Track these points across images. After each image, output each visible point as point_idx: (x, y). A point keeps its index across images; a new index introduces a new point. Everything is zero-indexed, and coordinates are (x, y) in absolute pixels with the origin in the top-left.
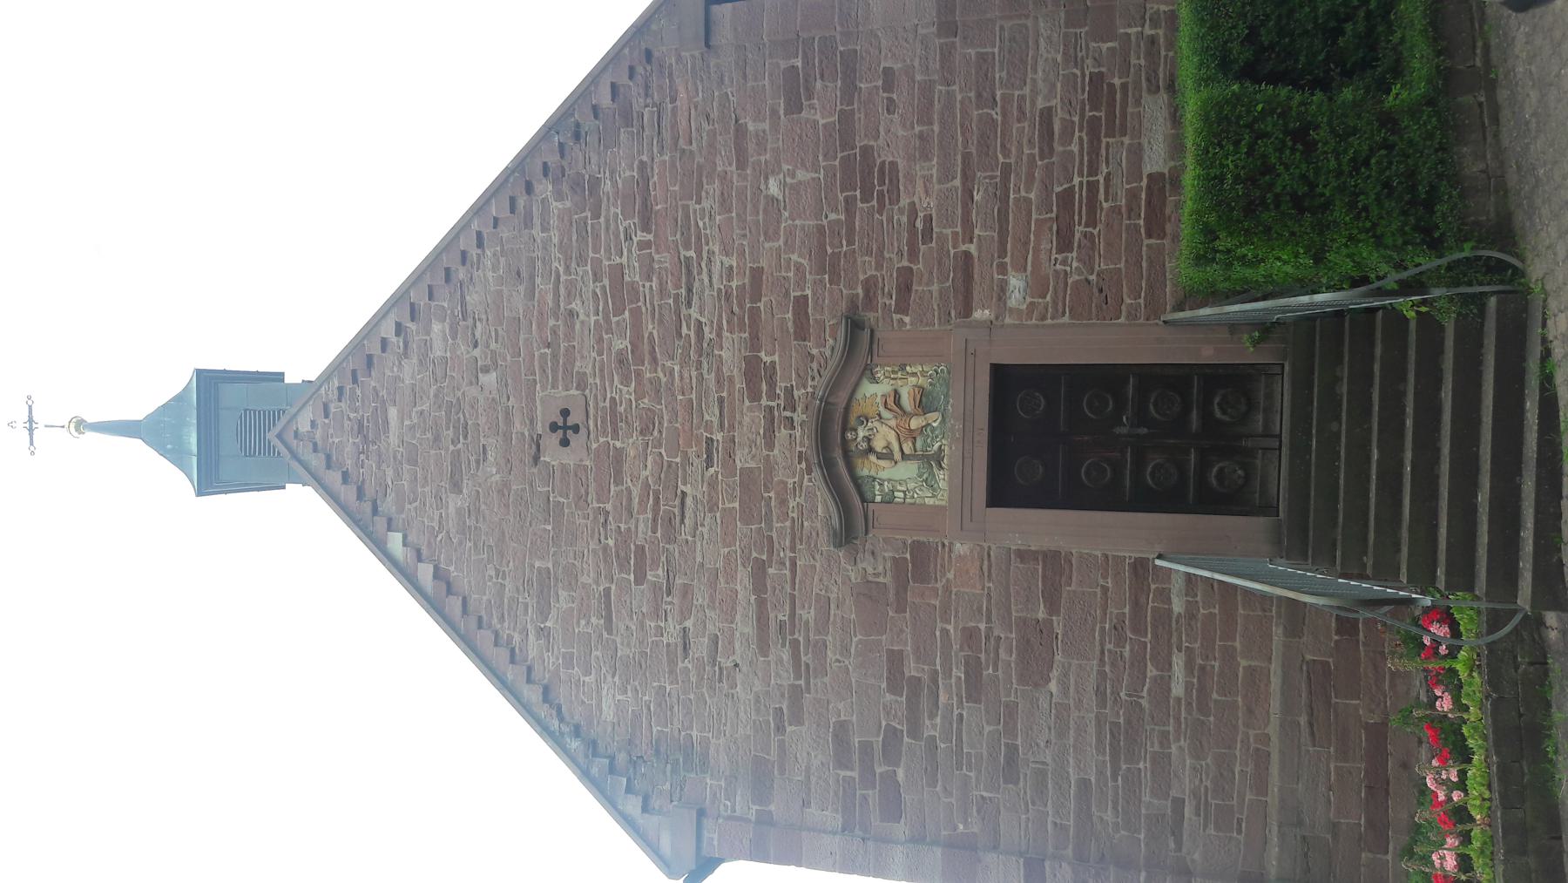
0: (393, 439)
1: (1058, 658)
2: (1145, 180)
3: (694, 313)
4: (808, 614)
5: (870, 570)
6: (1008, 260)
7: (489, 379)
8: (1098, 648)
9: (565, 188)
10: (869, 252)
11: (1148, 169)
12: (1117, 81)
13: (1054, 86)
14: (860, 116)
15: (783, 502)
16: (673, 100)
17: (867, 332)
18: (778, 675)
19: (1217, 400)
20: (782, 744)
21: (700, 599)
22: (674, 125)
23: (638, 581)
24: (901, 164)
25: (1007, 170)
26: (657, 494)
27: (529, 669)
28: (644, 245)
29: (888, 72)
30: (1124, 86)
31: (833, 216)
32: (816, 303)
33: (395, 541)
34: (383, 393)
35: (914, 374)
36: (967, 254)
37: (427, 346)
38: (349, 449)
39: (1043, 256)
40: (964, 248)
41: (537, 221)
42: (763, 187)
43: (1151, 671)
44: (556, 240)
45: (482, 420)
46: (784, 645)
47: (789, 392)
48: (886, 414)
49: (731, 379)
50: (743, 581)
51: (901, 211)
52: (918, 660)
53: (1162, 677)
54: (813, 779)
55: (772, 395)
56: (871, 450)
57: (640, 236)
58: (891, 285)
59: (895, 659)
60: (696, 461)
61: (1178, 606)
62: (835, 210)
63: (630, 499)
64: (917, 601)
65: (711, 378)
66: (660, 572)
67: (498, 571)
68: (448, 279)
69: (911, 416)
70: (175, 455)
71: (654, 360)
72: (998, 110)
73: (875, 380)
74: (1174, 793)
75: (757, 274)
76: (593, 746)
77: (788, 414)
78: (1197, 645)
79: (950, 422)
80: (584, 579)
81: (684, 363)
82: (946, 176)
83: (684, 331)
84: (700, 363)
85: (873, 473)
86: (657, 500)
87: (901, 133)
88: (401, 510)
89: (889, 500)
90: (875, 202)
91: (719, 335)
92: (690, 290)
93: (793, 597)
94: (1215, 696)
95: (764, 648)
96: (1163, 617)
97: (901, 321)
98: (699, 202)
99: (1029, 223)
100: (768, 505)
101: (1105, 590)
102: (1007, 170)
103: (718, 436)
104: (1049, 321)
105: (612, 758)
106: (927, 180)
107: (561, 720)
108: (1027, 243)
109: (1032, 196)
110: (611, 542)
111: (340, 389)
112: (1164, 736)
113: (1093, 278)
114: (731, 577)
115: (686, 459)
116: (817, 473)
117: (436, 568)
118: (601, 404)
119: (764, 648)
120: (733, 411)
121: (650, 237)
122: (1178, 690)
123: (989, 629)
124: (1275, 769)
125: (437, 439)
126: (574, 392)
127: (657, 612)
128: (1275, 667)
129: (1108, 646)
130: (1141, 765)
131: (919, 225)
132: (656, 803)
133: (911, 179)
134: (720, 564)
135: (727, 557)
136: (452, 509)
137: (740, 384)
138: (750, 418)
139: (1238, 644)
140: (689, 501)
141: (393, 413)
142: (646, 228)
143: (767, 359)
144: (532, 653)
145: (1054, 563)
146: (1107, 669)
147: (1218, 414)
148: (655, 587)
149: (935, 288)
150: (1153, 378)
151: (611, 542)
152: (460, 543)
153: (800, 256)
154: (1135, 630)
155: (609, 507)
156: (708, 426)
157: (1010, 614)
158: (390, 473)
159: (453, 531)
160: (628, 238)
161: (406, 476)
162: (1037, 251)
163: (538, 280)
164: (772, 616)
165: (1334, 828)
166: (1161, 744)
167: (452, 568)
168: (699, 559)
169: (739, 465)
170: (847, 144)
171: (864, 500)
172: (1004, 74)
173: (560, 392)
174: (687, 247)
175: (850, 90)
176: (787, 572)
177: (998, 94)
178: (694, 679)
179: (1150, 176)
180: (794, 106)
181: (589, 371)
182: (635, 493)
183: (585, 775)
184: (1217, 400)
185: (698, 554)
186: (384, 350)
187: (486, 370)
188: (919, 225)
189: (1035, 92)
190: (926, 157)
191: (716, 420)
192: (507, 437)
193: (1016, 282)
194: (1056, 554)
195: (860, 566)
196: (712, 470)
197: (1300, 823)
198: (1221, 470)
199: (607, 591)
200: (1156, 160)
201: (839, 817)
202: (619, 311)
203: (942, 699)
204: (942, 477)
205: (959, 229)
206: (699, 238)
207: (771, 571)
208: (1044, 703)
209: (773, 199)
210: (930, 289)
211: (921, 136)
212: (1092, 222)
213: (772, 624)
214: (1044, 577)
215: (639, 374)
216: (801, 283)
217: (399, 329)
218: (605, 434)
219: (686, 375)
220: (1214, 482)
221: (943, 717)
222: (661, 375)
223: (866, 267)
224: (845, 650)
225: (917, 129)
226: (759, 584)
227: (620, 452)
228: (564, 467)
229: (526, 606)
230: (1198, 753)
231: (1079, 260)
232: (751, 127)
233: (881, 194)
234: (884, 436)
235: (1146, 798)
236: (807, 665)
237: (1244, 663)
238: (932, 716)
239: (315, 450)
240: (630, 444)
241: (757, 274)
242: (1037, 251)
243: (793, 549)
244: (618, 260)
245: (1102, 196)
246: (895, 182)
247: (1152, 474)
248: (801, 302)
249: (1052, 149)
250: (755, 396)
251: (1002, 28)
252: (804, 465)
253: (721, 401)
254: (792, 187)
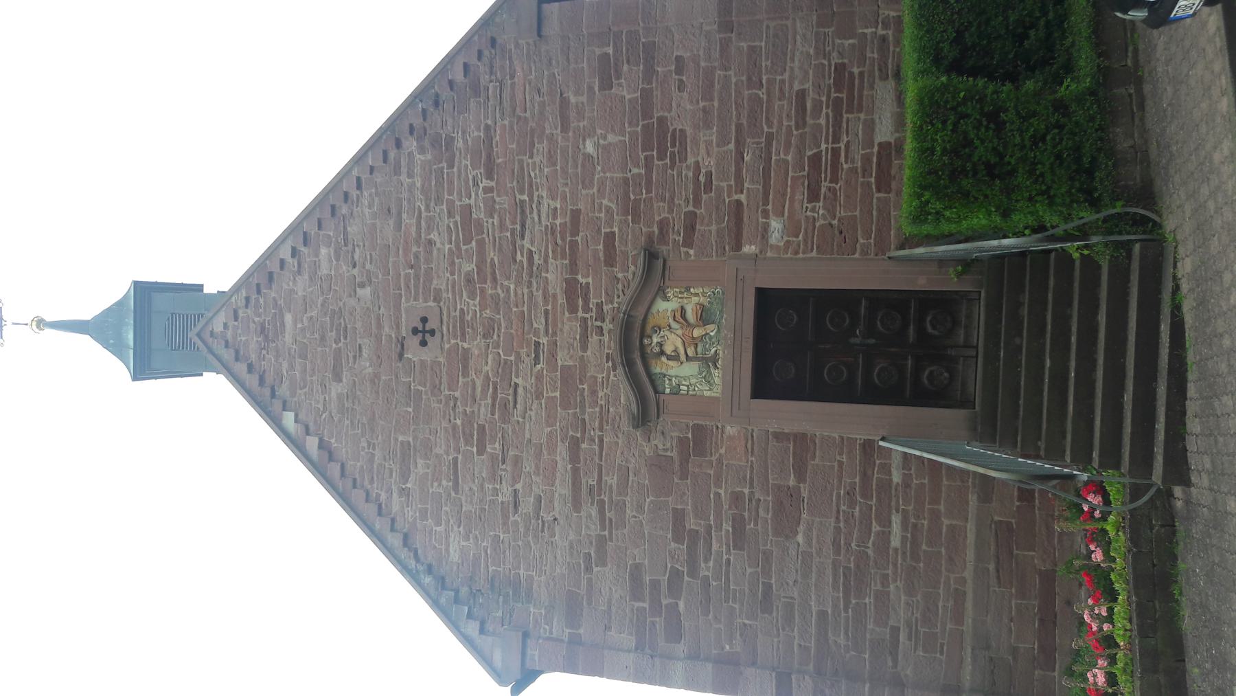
0: (288, 338)
1: (804, 516)
2: (876, 149)
3: (527, 244)
4: (612, 480)
5: (660, 446)
6: (770, 207)
7: (365, 293)
8: (834, 508)
9: (427, 144)
10: (663, 199)
11: (879, 139)
12: (856, 70)
13: (807, 73)
14: (657, 94)
15: (594, 393)
16: (512, 77)
17: (660, 262)
18: (588, 527)
19: (929, 319)
20: (590, 580)
21: (528, 467)
22: (513, 97)
23: (480, 453)
24: (689, 131)
25: (770, 137)
26: (495, 384)
27: (393, 520)
28: (487, 190)
29: (679, 59)
30: (861, 74)
31: (635, 171)
32: (621, 237)
33: (289, 419)
34: (281, 302)
35: (697, 295)
36: (739, 203)
37: (316, 266)
38: (253, 346)
39: (797, 205)
40: (736, 197)
41: (404, 170)
42: (581, 147)
43: (876, 527)
44: (419, 185)
45: (359, 325)
46: (592, 504)
47: (600, 306)
48: (674, 325)
49: (554, 296)
50: (562, 451)
51: (688, 167)
52: (696, 516)
53: (883, 532)
54: (614, 610)
55: (586, 309)
56: (662, 353)
57: (485, 183)
58: (679, 225)
59: (679, 517)
60: (527, 360)
61: (896, 477)
62: (637, 166)
63: (474, 388)
64: (697, 470)
65: (539, 295)
66: (497, 445)
67: (369, 444)
68: (333, 214)
69: (694, 327)
70: (116, 349)
71: (495, 280)
72: (764, 90)
73: (666, 299)
74: (891, 623)
75: (576, 214)
76: (442, 582)
77: (599, 324)
78: (911, 508)
79: (724, 332)
80: (439, 450)
81: (518, 282)
82: (723, 141)
83: (519, 257)
84: (530, 283)
85: (664, 371)
86: (495, 389)
87: (689, 107)
88: (293, 394)
89: (676, 392)
90: (668, 161)
91: (546, 261)
92: (523, 226)
93: (600, 467)
94: (924, 547)
96: (885, 486)
97: (687, 253)
98: (531, 157)
99: (787, 179)
100: (582, 395)
101: (841, 463)
102: (770, 137)
103: (544, 340)
104: (801, 255)
105: (457, 591)
106: (709, 144)
107: (417, 559)
108: (784, 195)
109: (789, 158)
110: (459, 422)
111: (247, 299)
112: (885, 577)
113: (835, 222)
114: (552, 451)
115: (518, 355)
116: (620, 370)
117: (321, 440)
118: (453, 314)
120: (555, 321)
121: (493, 184)
122: (895, 542)
123: (752, 493)
124: (969, 605)
125: (323, 338)
126: (431, 304)
127: (493, 477)
128: (971, 527)
129: (843, 508)
130: (867, 600)
131: (702, 179)
132: (490, 627)
133: (696, 142)
134: (544, 440)
135: (550, 435)
136: (333, 394)
137: (561, 299)
138: (569, 327)
139: (942, 508)
140: (520, 390)
141: (288, 318)
142: (489, 176)
143: (583, 281)
144: (396, 507)
145: (802, 442)
146: (842, 525)
147: (930, 329)
148: (493, 458)
149: (714, 228)
150: (880, 301)
151: (459, 422)
152: (340, 421)
153: (610, 200)
154: (864, 496)
155: (457, 394)
156: (536, 332)
157: (767, 481)
158: (285, 365)
159: (334, 411)
160: (476, 184)
161: (298, 367)
162: (792, 201)
163: (404, 216)
164: (583, 481)
165: (1014, 651)
166: (882, 583)
167: (333, 441)
168: (527, 436)
169: (560, 363)
170: (647, 114)
171: (656, 392)
172: (769, 63)
173: (421, 304)
174: (522, 192)
175: (649, 73)
176: (596, 447)
177: (764, 78)
178: (522, 530)
179: (880, 144)
180: (606, 84)
181: (443, 287)
182: (479, 383)
183: (435, 604)
184: (929, 319)
185: (527, 432)
186: (282, 268)
187: (362, 285)
188: (702, 179)
189: (792, 78)
190: (708, 126)
191: (542, 328)
192: (378, 339)
193: (776, 225)
194: (804, 435)
195: (653, 442)
196: (539, 367)
197: (988, 647)
198: (931, 373)
199: (455, 460)
200: (884, 132)
201: (633, 638)
202: (468, 241)
203: (715, 547)
204: (717, 375)
205: (733, 183)
206: (531, 185)
207: (583, 446)
208: (792, 552)
209: (588, 157)
210: (710, 228)
211: (704, 110)
212: (835, 180)
213: (584, 487)
214: (794, 453)
215: (482, 291)
216: (610, 222)
217: (294, 252)
218: (455, 337)
219: (520, 292)
220: (926, 382)
221: (716, 561)
222: (500, 291)
223: (661, 211)
224: (640, 508)
225: (702, 104)
226: (574, 457)
227: (466, 351)
228: (423, 362)
229: (391, 471)
230: (910, 591)
231: (824, 208)
232: (573, 100)
233: (673, 154)
234: (673, 342)
235: (870, 626)
236: (611, 520)
237: (946, 522)
238: (706, 560)
239: (227, 346)
240: (475, 345)
241: (576, 214)
242: (792, 201)
243: (601, 429)
244: (467, 201)
245: (842, 159)
246: (683, 145)
247: (879, 375)
248: (610, 237)
249: (805, 123)
250: (573, 309)
251: (768, 27)
252: (610, 364)
253: (546, 312)
254: (604, 147)
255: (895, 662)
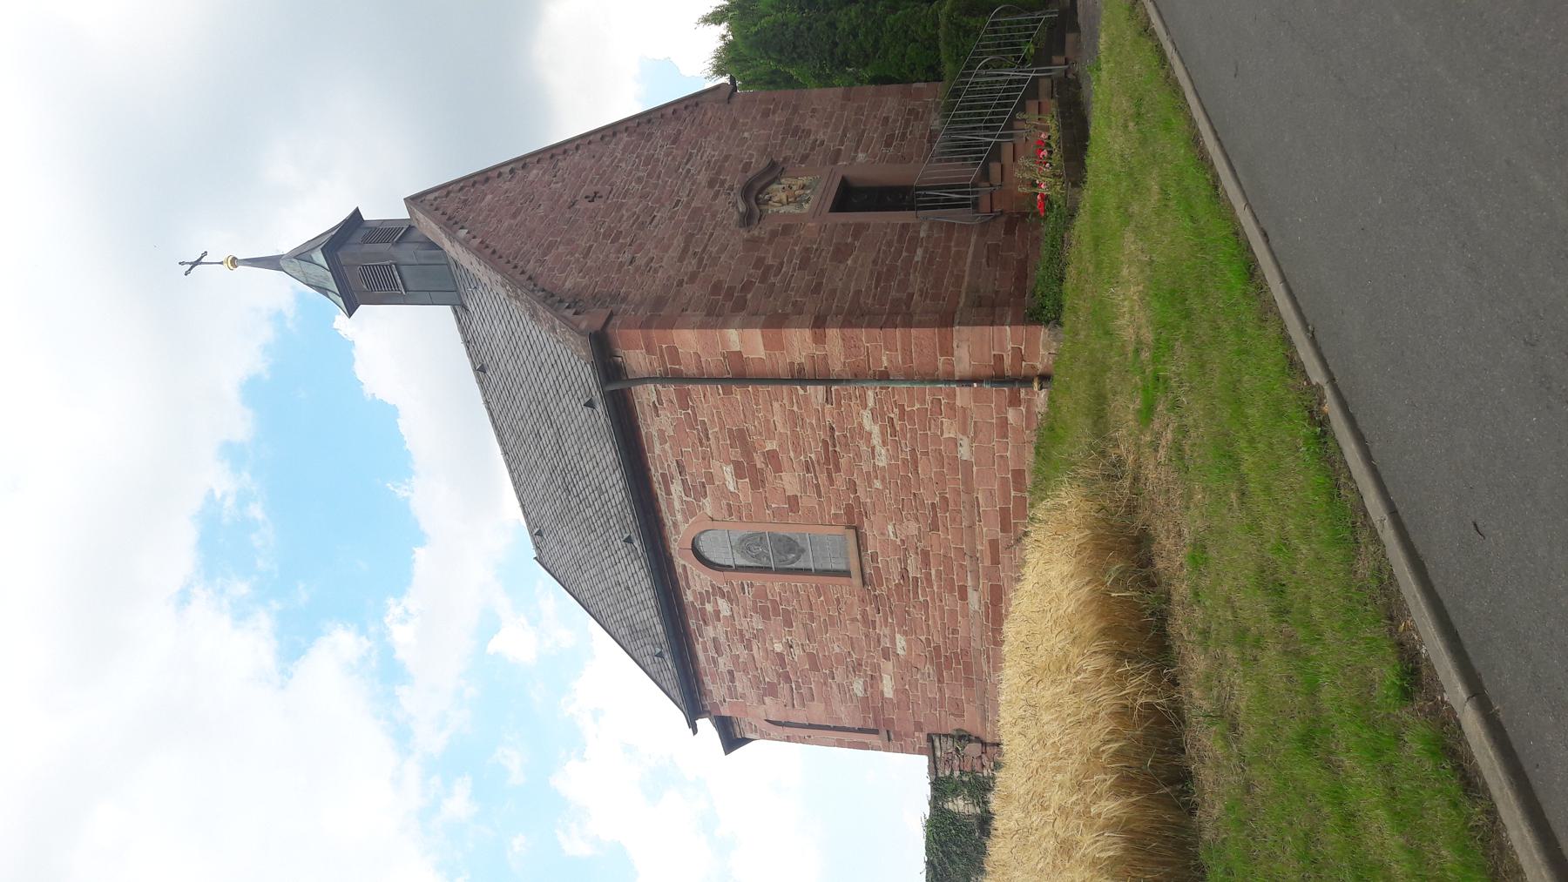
15: (714, 216)
59: (760, 260)
61: (922, 234)
75: (727, 158)
95: (681, 259)
119: (681, 259)
128: (972, 249)
193: (861, 156)
216: (751, 156)
255: (908, 307)
